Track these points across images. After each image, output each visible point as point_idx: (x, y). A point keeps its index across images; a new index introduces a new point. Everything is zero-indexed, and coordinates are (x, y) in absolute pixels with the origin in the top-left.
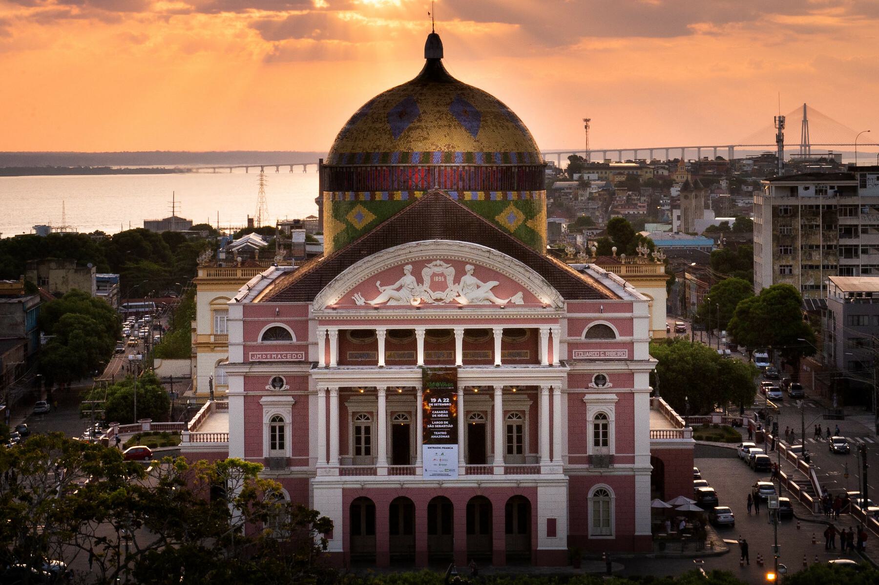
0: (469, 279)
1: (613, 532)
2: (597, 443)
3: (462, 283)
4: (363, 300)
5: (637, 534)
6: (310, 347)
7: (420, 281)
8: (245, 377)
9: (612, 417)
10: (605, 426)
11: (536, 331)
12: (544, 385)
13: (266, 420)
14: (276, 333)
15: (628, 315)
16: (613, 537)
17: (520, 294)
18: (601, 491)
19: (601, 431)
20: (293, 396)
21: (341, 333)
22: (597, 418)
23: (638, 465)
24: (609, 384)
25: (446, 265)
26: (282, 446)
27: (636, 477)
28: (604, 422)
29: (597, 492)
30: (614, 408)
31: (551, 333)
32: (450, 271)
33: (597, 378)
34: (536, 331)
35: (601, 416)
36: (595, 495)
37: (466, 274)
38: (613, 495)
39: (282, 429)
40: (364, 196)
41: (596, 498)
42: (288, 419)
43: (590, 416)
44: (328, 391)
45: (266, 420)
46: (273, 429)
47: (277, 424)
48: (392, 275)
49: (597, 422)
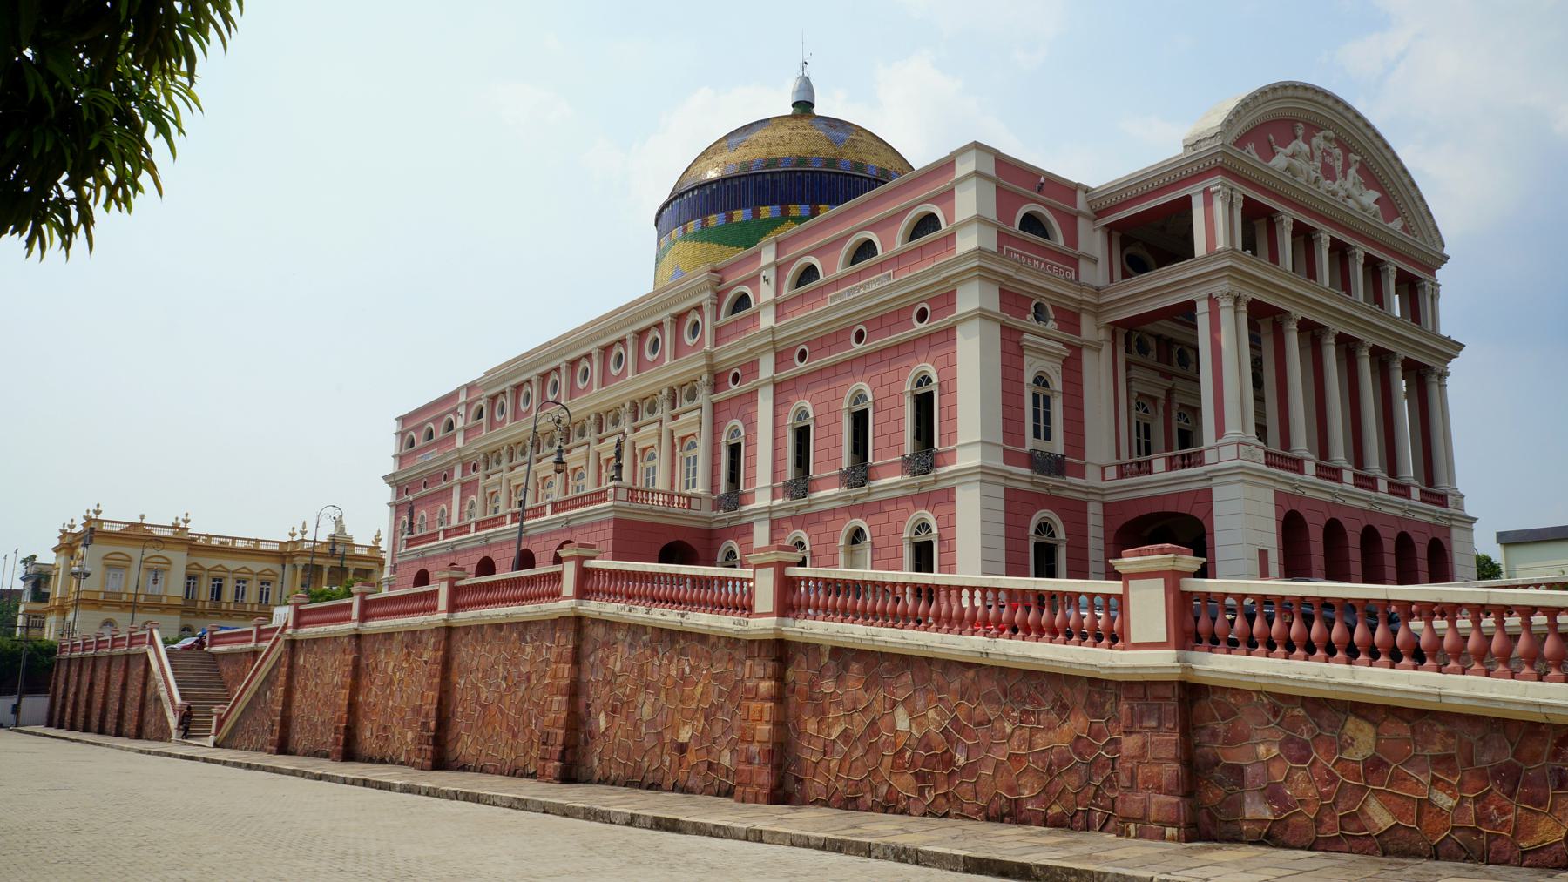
3: (1350, 178)
4: (1256, 157)
6: (1083, 265)
8: (1002, 292)
13: (1029, 378)
14: (1032, 223)
20: (1065, 344)
21: (1247, 200)
26: (1048, 437)
32: (1338, 151)
39: (1047, 399)
40: (795, 210)
42: (1057, 384)
44: (1237, 300)
45: (1029, 378)
46: (1036, 397)
47: (1042, 391)
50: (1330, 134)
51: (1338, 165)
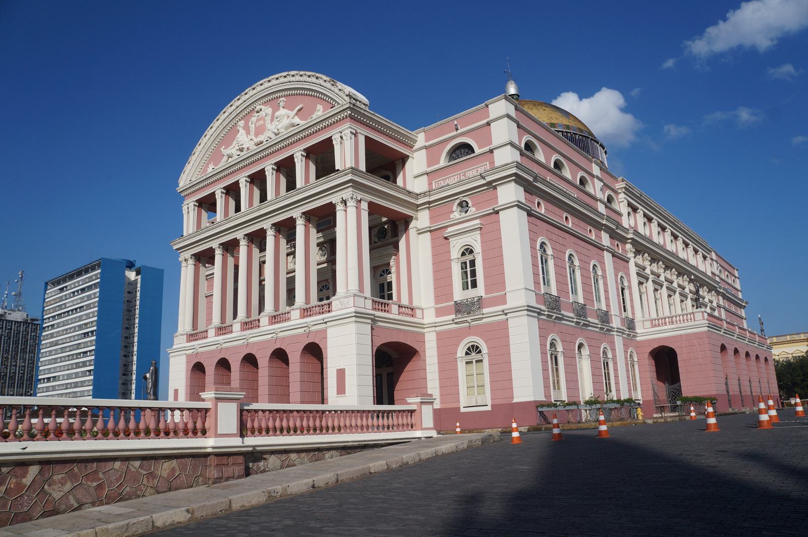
0: (282, 112)
1: (489, 403)
2: (465, 287)
5: (515, 400)
7: (248, 133)
9: (478, 248)
10: (473, 263)
11: (329, 140)
12: (335, 199)
15: (485, 121)
16: (489, 408)
17: (320, 107)
18: (473, 346)
19: (469, 269)
22: (463, 254)
23: (511, 303)
24: (472, 210)
25: (263, 107)
27: (511, 323)
28: (470, 257)
29: (469, 349)
30: (478, 237)
31: (341, 137)
33: (460, 205)
34: (329, 140)
35: (469, 251)
36: (467, 354)
37: (278, 109)
38: (485, 350)
41: (469, 358)
43: (455, 253)
44: (186, 260)
48: (230, 134)
49: (464, 259)
50: (258, 108)
51: (268, 118)
